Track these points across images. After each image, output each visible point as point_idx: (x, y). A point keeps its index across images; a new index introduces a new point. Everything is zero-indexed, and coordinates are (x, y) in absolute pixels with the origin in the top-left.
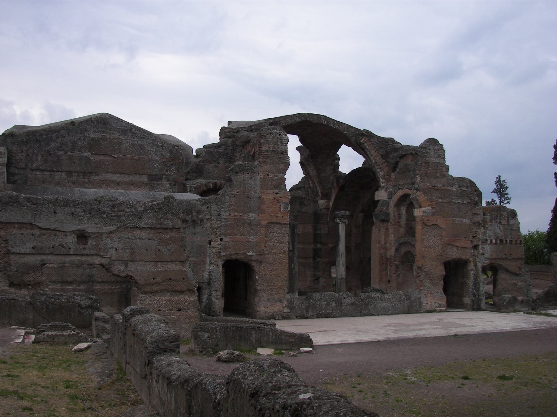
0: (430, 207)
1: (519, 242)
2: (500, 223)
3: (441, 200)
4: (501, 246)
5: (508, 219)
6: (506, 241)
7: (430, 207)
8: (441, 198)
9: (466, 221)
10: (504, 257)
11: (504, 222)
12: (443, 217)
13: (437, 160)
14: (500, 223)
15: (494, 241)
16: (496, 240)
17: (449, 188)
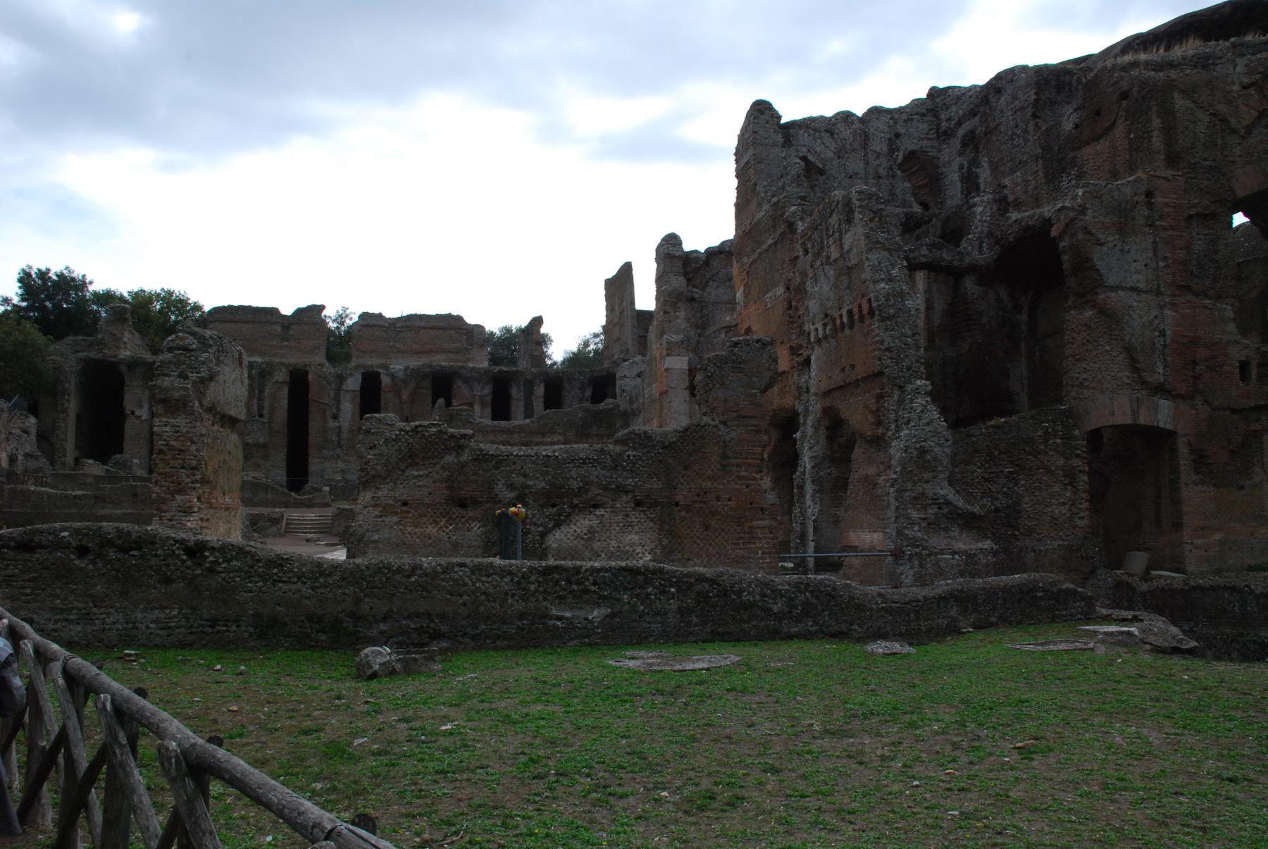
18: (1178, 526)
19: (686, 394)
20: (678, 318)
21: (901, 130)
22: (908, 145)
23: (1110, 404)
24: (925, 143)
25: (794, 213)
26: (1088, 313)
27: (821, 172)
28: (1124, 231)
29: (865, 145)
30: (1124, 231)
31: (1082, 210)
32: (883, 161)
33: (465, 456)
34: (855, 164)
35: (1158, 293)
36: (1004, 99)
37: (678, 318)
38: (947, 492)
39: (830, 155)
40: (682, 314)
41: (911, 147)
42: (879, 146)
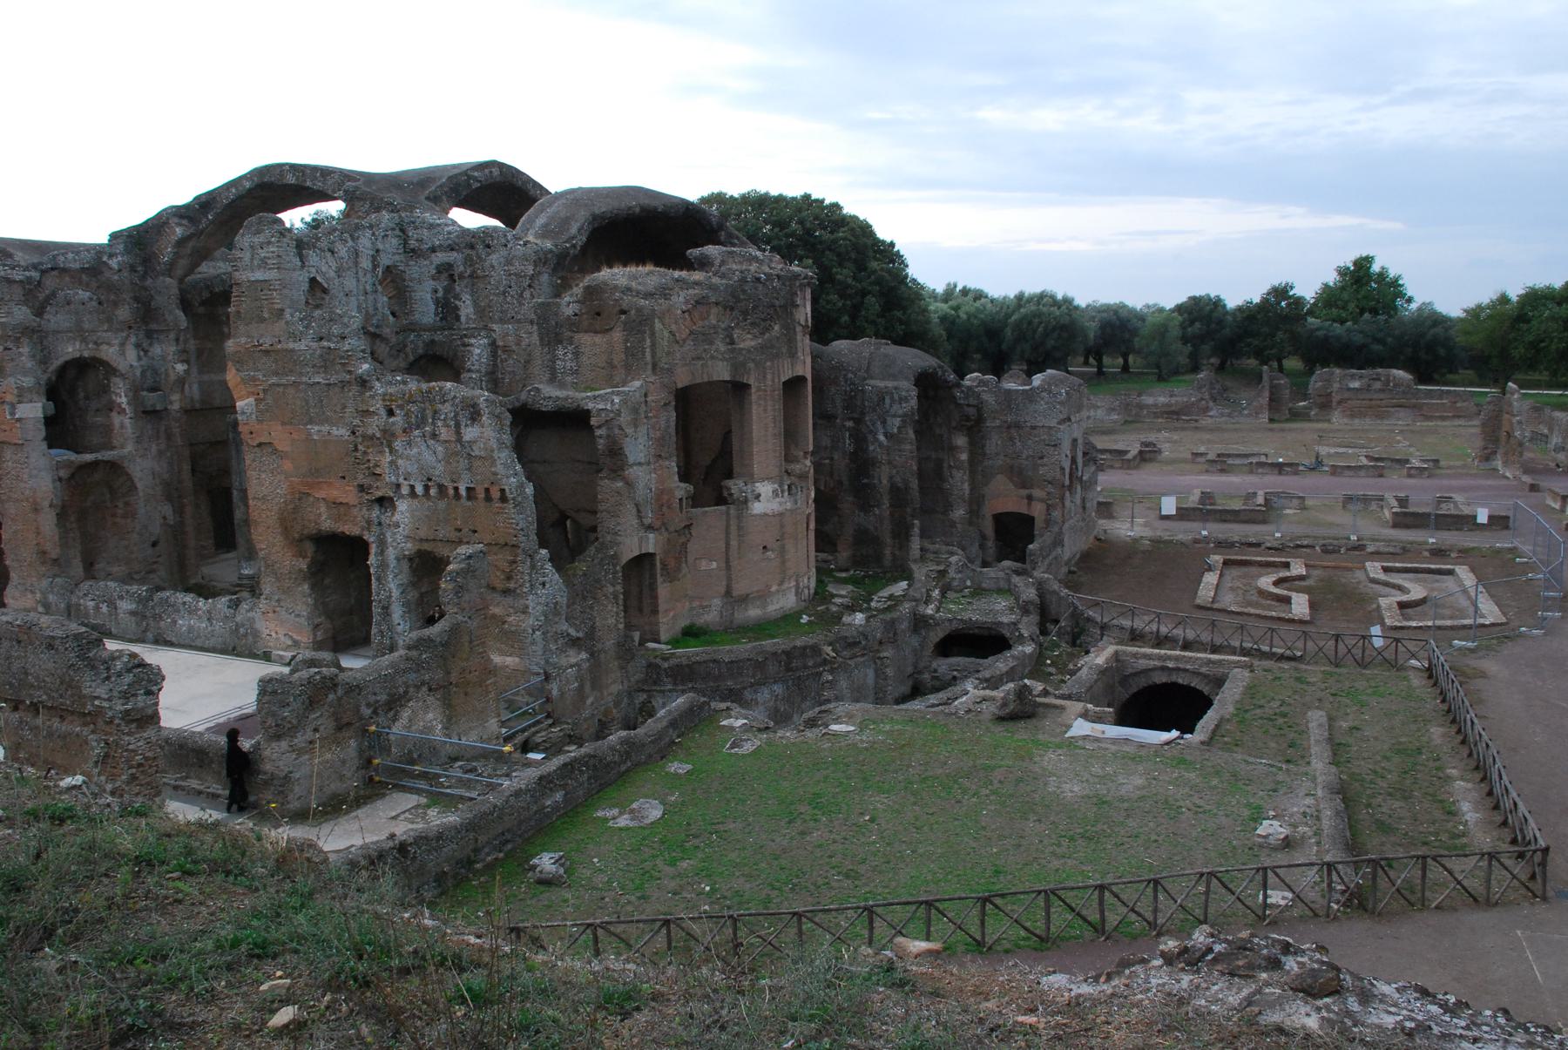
0: (251, 400)
1: (496, 494)
2: (434, 436)
3: (274, 380)
4: (442, 504)
5: (458, 425)
6: (456, 489)
7: (251, 400)
8: (276, 374)
9: (341, 432)
10: (454, 535)
11: (445, 433)
12: (283, 424)
13: (259, 275)
14: (434, 436)
15: (419, 490)
16: (427, 488)
17: (291, 345)
18: (655, 612)
19: (44, 446)
20: (21, 354)
21: (381, 247)
22: (385, 260)
23: (632, 543)
24: (397, 257)
25: (368, 372)
26: (620, 484)
27: (325, 291)
28: (636, 426)
29: (356, 263)
30: (635, 424)
31: (619, 413)
32: (369, 275)
33: (340, 692)
34: (350, 283)
35: (649, 463)
36: (495, 258)
37: (21, 354)
38: (564, 627)
39: (332, 274)
40: (25, 350)
41: (388, 263)
42: (366, 263)
